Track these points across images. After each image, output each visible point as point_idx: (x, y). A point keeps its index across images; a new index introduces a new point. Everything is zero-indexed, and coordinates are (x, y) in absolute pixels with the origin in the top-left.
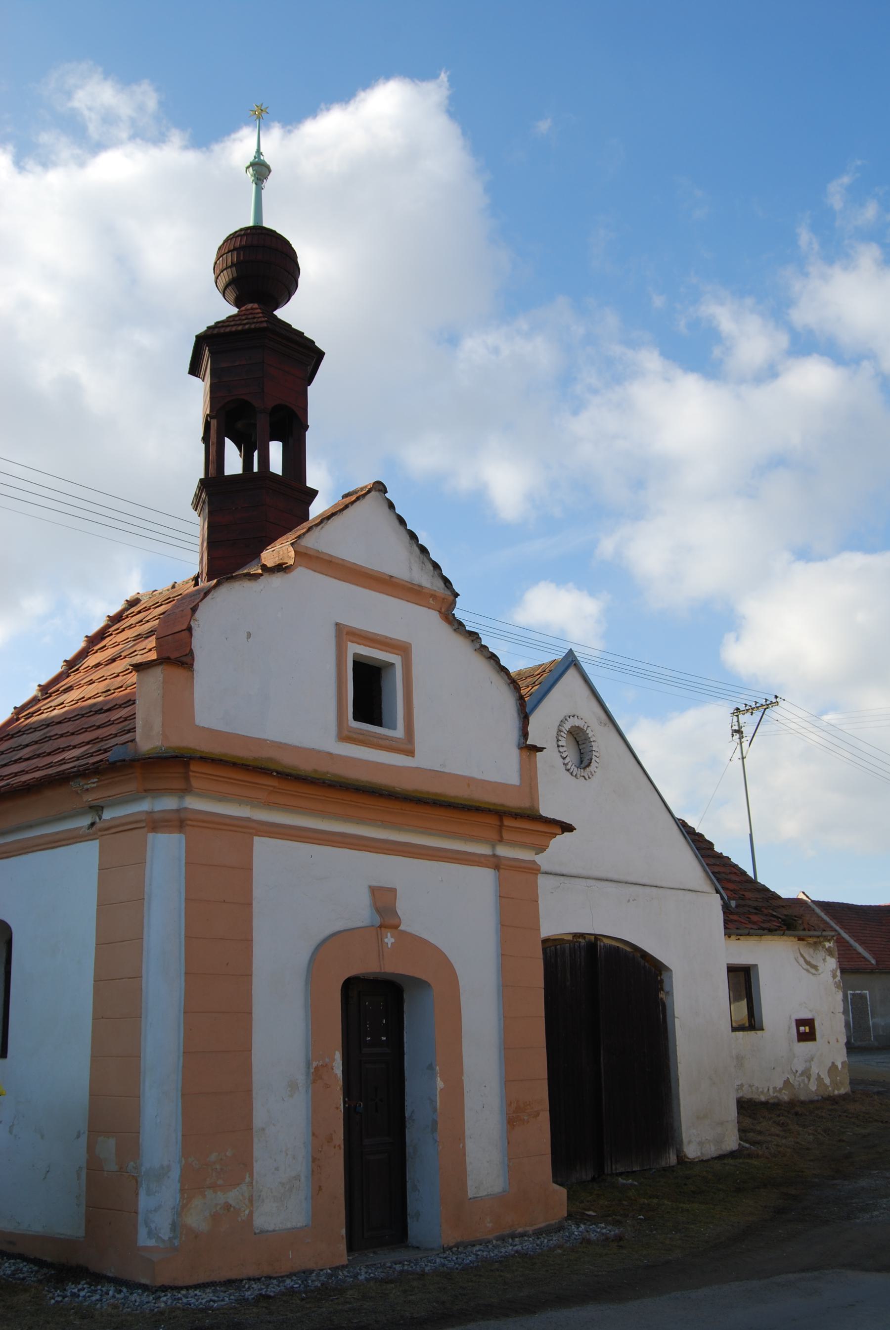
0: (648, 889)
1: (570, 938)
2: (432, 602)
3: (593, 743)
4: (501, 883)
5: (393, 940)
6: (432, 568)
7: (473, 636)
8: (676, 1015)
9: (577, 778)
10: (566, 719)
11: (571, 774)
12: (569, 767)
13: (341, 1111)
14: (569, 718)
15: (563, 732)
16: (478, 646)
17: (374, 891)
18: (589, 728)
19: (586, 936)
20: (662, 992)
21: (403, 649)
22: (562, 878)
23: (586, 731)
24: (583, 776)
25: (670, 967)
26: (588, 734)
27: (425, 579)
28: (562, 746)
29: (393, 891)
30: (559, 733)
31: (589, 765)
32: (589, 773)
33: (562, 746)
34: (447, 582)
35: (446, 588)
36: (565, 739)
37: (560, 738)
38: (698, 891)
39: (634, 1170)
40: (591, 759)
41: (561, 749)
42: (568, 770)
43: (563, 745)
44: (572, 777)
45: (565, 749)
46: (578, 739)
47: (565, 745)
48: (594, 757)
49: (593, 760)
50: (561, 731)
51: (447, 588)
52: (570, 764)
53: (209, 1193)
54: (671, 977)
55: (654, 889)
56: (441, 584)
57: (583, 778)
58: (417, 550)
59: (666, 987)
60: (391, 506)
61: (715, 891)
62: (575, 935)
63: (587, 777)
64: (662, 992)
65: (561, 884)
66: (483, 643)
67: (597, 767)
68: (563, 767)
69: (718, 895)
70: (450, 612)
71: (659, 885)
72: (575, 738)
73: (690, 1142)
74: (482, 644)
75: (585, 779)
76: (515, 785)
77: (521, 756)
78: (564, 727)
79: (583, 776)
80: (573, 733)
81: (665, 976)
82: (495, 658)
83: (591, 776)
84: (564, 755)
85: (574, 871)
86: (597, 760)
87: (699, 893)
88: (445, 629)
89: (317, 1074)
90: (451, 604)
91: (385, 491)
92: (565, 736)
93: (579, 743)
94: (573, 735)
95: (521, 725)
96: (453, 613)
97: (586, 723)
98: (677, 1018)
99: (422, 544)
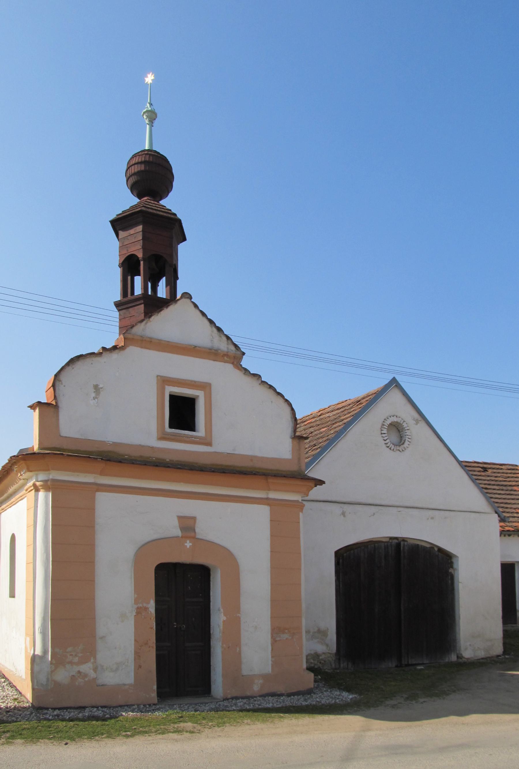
0: (442, 513)
1: (388, 540)
2: (227, 359)
3: (407, 431)
4: (272, 513)
5: (191, 544)
6: (226, 339)
7: (257, 376)
8: (460, 581)
9: (394, 451)
10: (388, 418)
11: (390, 449)
12: (388, 445)
13: (154, 629)
14: (390, 417)
15: (385, 425)
16: (260, 382)
17: (180, 518)
18: (405, 422)
19: (399, 539)
20: (451, 569)
21: (205, 387)
22: (380, 507)
23: (402, 424)
24: (399, 450)
25: (457, 555)
26: (403, 426)
27: (223, 346)
28: (384, 434)
29: (194, 519)
30: (383, 426)
31: (403, 444)
32: (403, 448)
33: (384, 434)
34: (236, 346)
35: (237, 350)
36: (386, 430)
37: (383, 429)
38: (480, 513)
39: (410, 663)
40: (405, 440)
41: (384, 435)
42: (388, 447)
43: (385, 433)
44: (391, 451)
45: (386, 435)
46: (399, 429)
47: (386, 432)
48: (407, 439)
49: (406, 441)
50: (384, 425)
51: (238, 350)
52: (389, 443)
53: (68, 666)
54: (458, 561)
55: (448, 512)
56: (233, 348)
57: (399, 451)
58: (215, 330)
59: (455, 566)
60: (196, 306)
61: (494, 512)
62: (391, 538)
63: (401, 450)
64: (451, 569)
65: (379, 510)
66: (263, 380)
67: (409, 445)
68: (384, 446)
69: (496, 514)
70: (238, 364)
71: (452, 509)
72: (397, 428)
73: (466, 649)
74: (262, 380)
75: (400, 451)
76: (287, 459)
77: (292, 442)
78: (385, 422)
79: (399, 450)
80: (396, 426)
81: (454, 560)
82: (272, 388)
83: (404, 450)
84: (385, 438)
85: (390, 503)
86: (409, 440)
87: (481, 514)
88: (239, 374)
89: (140, 611)
90: (240, 359)
91: (190, 297)
92: (387, 428)
93: (400, 431)
94: (396, 427)
95: (293, 425)
96: (241, 364)
97: (402, 419)
98: (461, 583)
99: (218, 326)
